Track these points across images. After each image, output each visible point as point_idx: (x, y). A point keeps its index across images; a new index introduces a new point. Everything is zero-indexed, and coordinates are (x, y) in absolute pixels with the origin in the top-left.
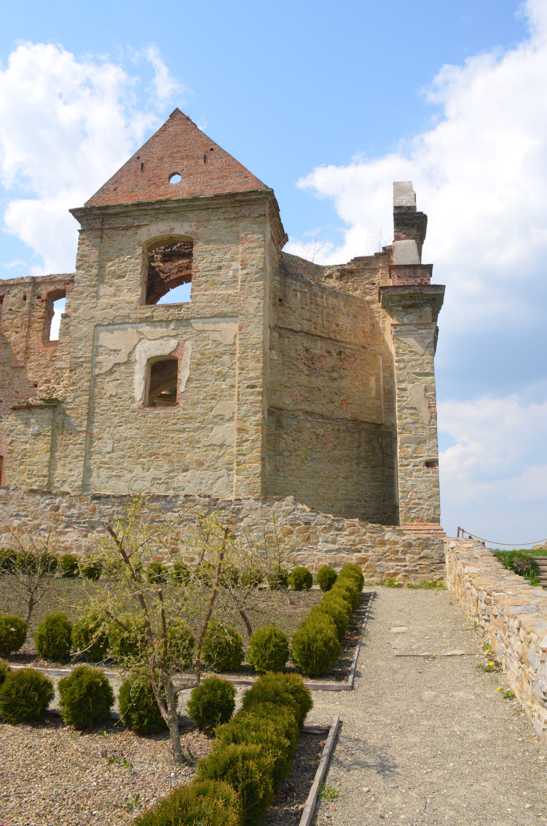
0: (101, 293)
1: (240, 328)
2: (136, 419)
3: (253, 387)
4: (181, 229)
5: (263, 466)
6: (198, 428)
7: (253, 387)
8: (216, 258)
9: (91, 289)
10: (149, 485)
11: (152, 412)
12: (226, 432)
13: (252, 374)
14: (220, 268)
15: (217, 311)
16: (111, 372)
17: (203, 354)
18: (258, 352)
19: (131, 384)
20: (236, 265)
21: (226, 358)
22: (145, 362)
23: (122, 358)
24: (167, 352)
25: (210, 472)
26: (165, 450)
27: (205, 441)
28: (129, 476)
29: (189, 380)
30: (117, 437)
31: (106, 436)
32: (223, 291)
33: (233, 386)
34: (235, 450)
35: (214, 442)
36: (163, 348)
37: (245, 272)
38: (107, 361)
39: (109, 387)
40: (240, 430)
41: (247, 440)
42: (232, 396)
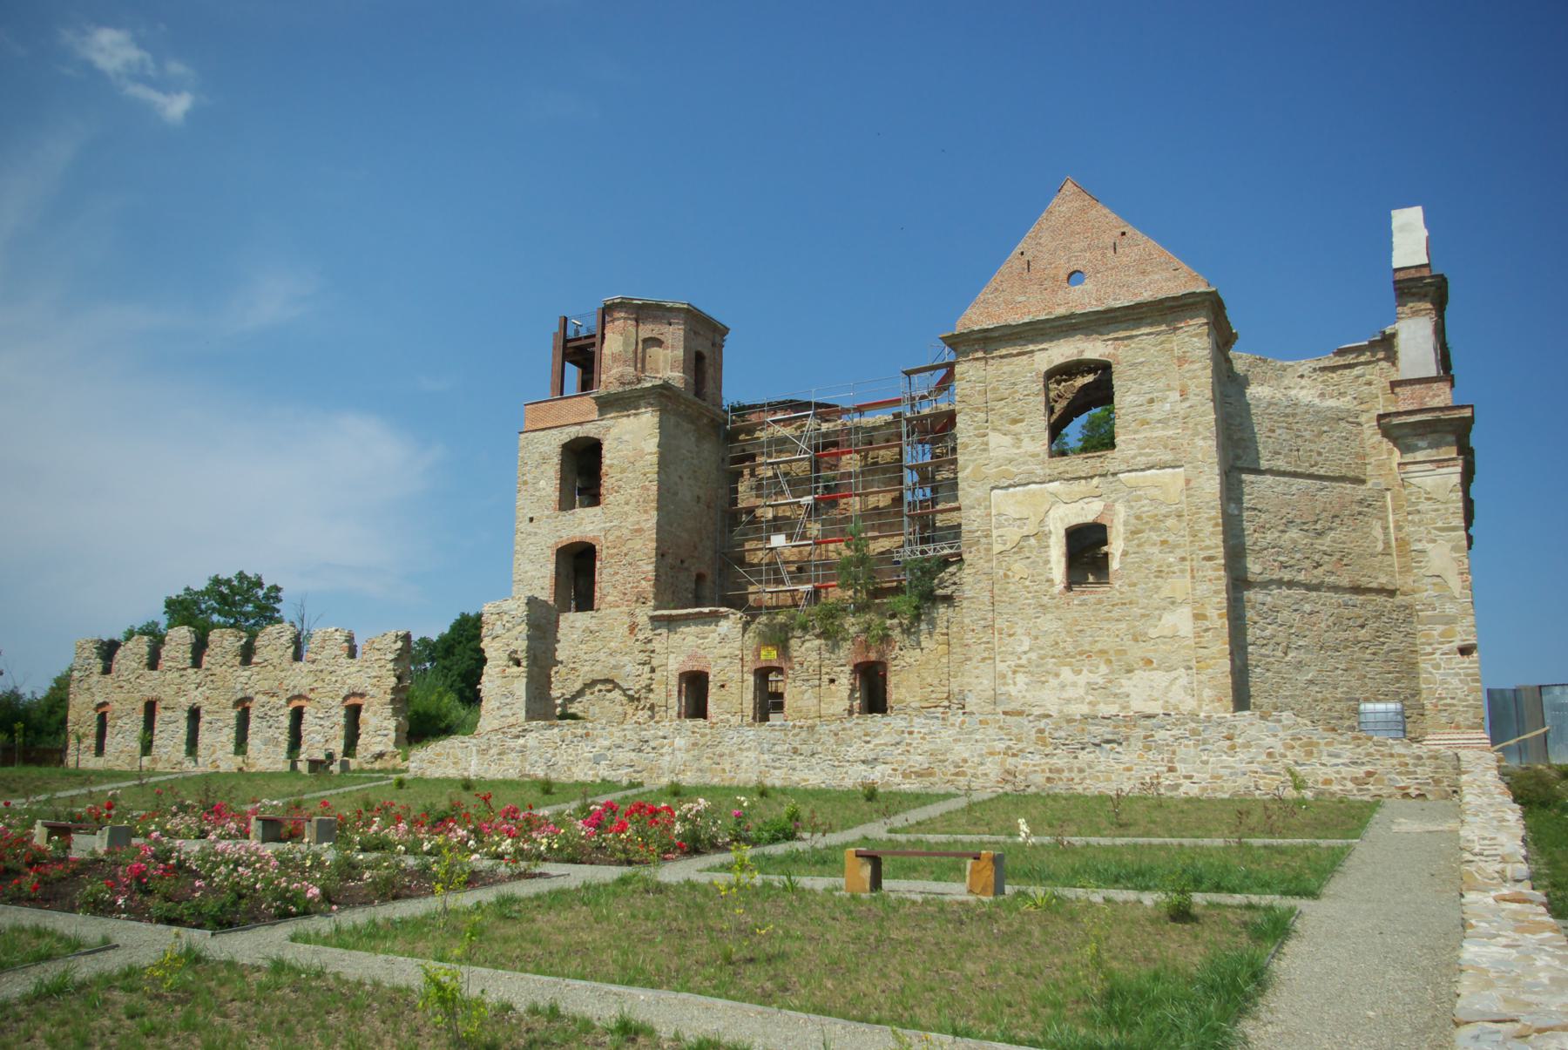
0: (992, 445)
1: (1188, 481)
2: (1057, 607)
3: (1209, 559)
4: (1093, 349)
5: (1232, 660)
6: (1143, 616)
7: (1209, 559)
8: (1145, 388)
9: (980, 440)
10: (1082, 692)
11: (1076, 596)
12: (1180, 621)
13: (1208, 543)
14: (1151, 401)
15: (1153, 459)
16: (1018, 548)
17: (1138, 518)
18: (1213, 513)
19: (1047, 562)
20: (1175, 396)
21: (1170, 522)
22: (1062, 533)
23: (1029, 529)
24: (1090, 519)
25: (1160, 673)
26: (1099, 646)
27: (1153, 633)
28: (1053, 682)
29: (1125, 554)
30: (1034, 632)
31: (1020, 631)
32: (1160, 433)
33: (1183, 559)
34: (1191, 642)
35: (1165, 633)
36: (1087, 513)
37: (1187, 404)
38: (1013, 534)
39: (1019, 567)
40: (1198, 617)
41: (1207, 630)
42: (1182, 571)
